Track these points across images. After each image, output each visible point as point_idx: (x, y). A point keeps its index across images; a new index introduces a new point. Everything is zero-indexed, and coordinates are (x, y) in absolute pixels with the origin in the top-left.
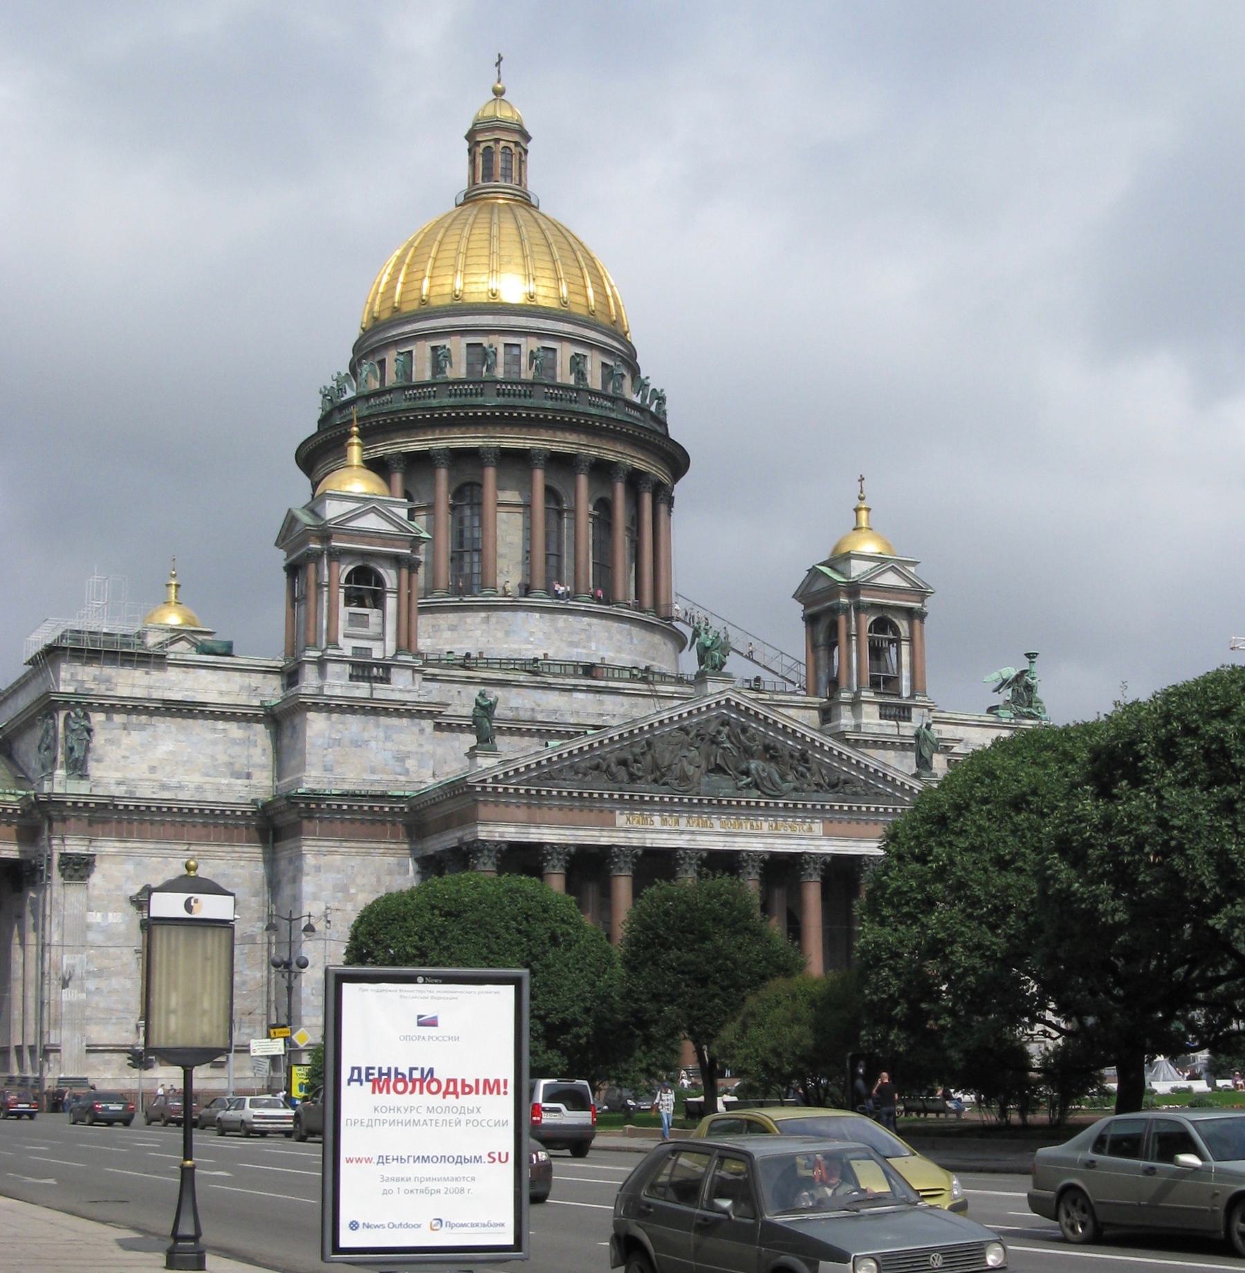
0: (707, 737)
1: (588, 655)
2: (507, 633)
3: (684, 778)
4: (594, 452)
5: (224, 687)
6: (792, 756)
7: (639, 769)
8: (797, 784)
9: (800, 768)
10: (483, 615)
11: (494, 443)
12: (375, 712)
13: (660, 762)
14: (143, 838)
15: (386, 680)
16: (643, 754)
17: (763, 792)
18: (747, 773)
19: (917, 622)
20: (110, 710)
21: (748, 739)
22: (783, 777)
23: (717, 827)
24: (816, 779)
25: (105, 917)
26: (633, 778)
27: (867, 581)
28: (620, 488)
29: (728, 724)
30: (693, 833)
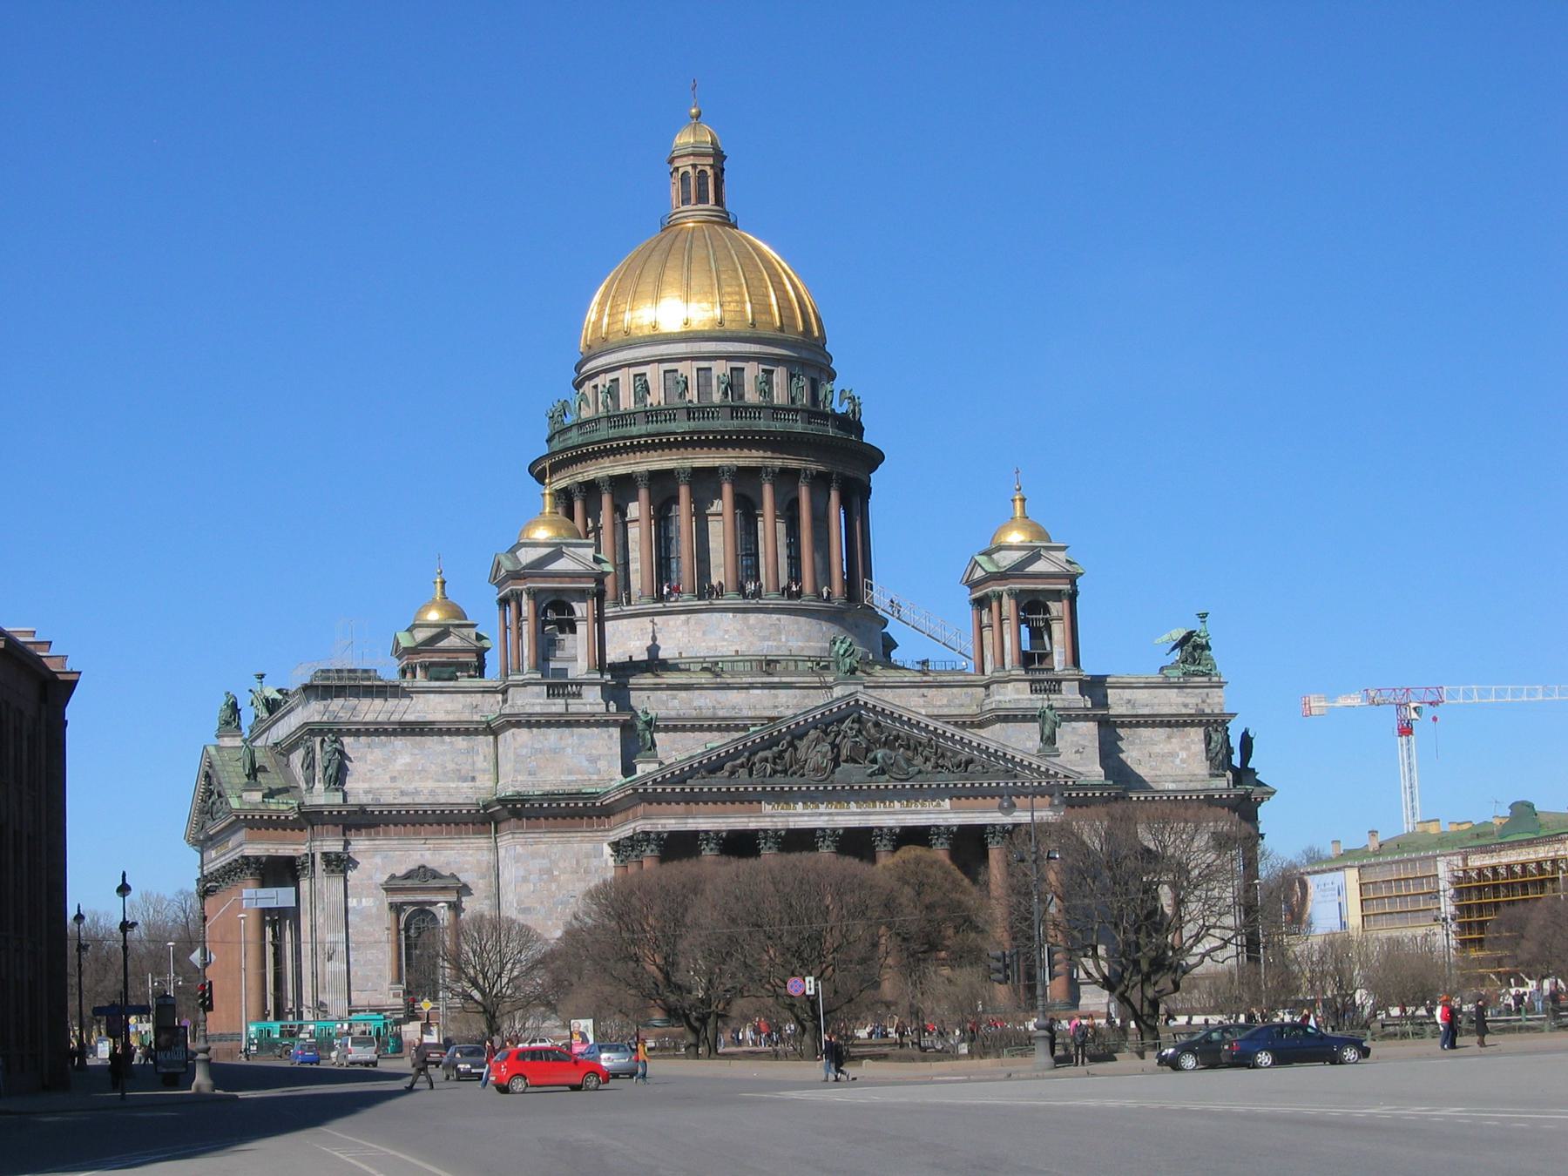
1: (778, 648)
2: (704, 633)
3: (816, 770)
4: (778, 463)
5: (449, 707)
10: (683, 617)
11: (688, 464)
12: (568, 724)
14: (387, 836)
15: (579, 695)
18: (874, 761)
20: (357, 733)
22: (909, 761)
23: (853, 807)
25: (360, 902)
26: (775, 772)
28: (804, 494)
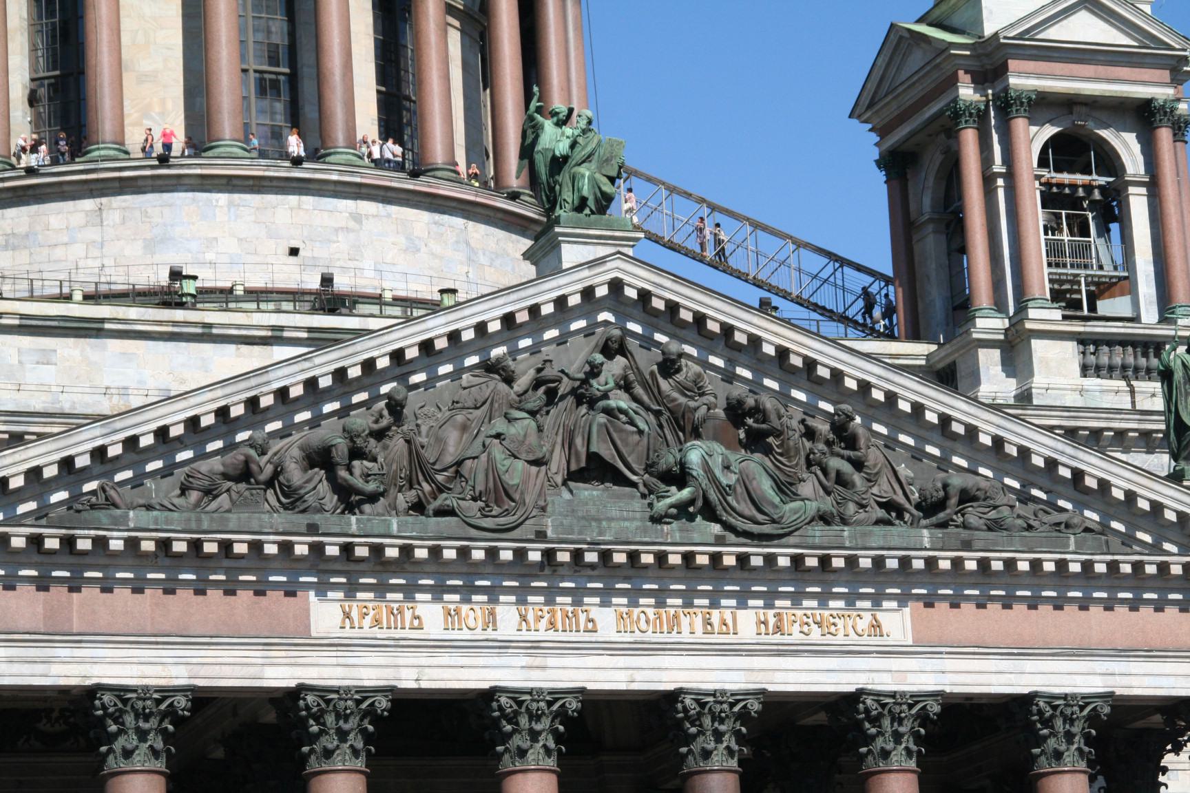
0: (565, 386)
2: (151, 246)
3: (499, 493)
6: (810, 434)
7: (366, 476)
8: (828, 504)
9: (835, 463)
10: (88, 204)
13: (429, 455)
16: (379, 435)
17: (727, 527)
18: (680, 477)
19: (1164, 135)
21: (682, 389)
24: (884, 488)
26: (350, 499)
27: (1020, 36)
29: (622, 350)
30: (534, 646)
